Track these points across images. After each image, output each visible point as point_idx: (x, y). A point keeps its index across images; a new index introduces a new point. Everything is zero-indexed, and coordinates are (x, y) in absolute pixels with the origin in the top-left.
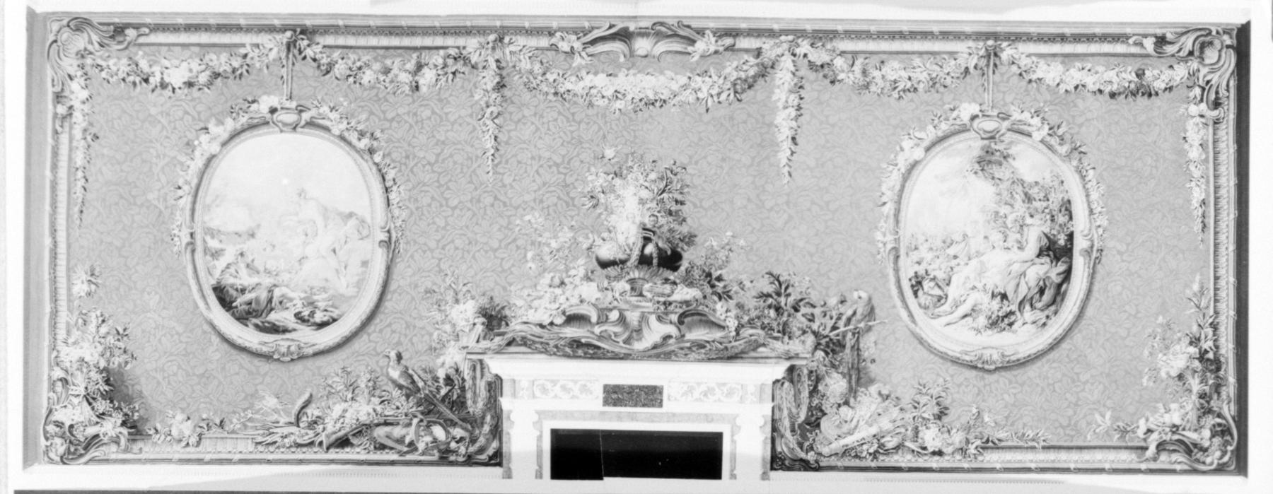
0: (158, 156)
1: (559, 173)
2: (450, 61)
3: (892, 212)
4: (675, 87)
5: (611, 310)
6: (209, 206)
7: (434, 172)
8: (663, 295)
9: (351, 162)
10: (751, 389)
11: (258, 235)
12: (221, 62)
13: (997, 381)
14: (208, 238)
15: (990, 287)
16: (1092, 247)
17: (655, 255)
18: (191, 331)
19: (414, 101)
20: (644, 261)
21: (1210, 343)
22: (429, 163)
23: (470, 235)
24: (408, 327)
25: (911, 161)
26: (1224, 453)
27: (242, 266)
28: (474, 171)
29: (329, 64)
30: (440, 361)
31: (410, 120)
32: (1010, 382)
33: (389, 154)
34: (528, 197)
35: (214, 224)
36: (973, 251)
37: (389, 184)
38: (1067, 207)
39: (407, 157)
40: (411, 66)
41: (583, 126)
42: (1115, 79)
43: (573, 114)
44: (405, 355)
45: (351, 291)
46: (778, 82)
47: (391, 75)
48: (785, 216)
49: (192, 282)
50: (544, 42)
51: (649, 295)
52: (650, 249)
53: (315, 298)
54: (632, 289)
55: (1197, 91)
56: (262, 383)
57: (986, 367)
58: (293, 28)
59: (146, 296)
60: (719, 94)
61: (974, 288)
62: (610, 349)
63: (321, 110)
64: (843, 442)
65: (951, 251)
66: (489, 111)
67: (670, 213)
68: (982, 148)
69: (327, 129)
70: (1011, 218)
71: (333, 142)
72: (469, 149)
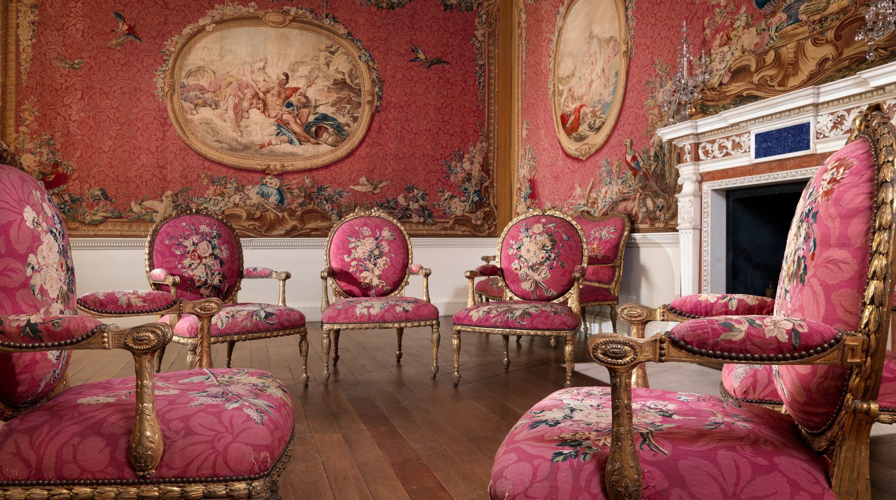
5: (767, 52)
8: (818, 11)
23: (669, 22)
30: (652, 141)
51: (803, 17)
54: (789, 17)
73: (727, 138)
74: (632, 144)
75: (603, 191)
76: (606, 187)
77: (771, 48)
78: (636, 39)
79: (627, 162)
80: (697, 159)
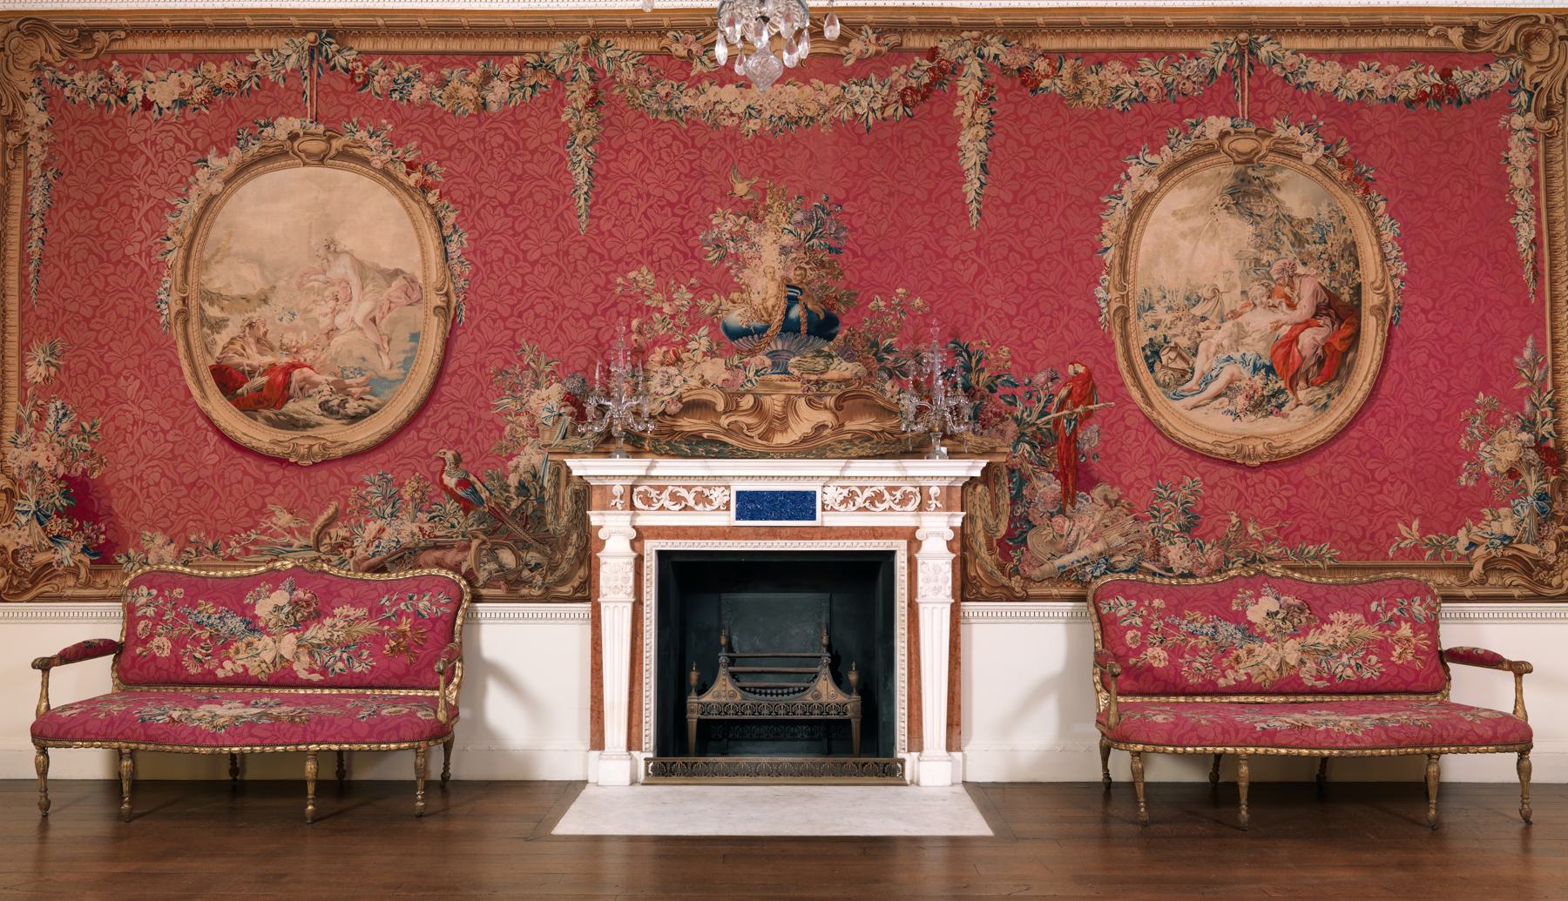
0: (141, 198)
1: (675, 215)
2: (528, 72)
3: (1117, 261)
4: (824, 100)
5: (743, 395)
6: (207, 263)
7: (507, 215)
9: (396, 202)
10: (934, 491)
11: (273, 301)
12: (225, 74)
13: (1263, 482)
14: (206, 305)
15: (1250, 356)
16: (1387, 303)
17: (803, 320)
18: (182, 427)
19: (480, 124)
20: (789, 327)
21: (1549, 427)
22: (501, 205)
23: (555, 297)
24: (471, 420)
25: (1141, 192)
27: (251, 340)
28: (561, 215)
29: (366, 76)
30: (512, 463)
31: (476, 149)
32: (1282, 483)
33: (448, 193)
34: (631, 248)
35: (216, 285)
36: (1227, 310)
37: (446, 232)
38: (1351, 251)
39: (472, 197)
40: (474, 77)
41: (706, 152)
42: (1413, 82)
43: (693, 138)
44: (467, 457)
45: (396, 373)
46: (960, 92)
48: (974, 268)
49: (184, 364)
50: (652, 45)
51: (796, 372)
52: (796, 312)
53: (347, 382)
54: (774, 364)
55: (1523, 97)
56: (271, 494)
57: (1248, 462)
58: (317, 29)
59: (122, 381)
60: (883, 108)
61: (1229, 359)
62: (742, 446)
64: (1058, 563)
65: (1197, 311)
66: (580, 136)
67: (822, 264)
68: (1236, 175)
69: (365, 161)
70: (1276, 266)
72: (554, 185)
73: (689, 488)
74: (458, 460)
75: (372, 527)
76: (380, 523)
77: (748, 392)
78: (472, 296)
79: (445, 488)
80: (632, 507)
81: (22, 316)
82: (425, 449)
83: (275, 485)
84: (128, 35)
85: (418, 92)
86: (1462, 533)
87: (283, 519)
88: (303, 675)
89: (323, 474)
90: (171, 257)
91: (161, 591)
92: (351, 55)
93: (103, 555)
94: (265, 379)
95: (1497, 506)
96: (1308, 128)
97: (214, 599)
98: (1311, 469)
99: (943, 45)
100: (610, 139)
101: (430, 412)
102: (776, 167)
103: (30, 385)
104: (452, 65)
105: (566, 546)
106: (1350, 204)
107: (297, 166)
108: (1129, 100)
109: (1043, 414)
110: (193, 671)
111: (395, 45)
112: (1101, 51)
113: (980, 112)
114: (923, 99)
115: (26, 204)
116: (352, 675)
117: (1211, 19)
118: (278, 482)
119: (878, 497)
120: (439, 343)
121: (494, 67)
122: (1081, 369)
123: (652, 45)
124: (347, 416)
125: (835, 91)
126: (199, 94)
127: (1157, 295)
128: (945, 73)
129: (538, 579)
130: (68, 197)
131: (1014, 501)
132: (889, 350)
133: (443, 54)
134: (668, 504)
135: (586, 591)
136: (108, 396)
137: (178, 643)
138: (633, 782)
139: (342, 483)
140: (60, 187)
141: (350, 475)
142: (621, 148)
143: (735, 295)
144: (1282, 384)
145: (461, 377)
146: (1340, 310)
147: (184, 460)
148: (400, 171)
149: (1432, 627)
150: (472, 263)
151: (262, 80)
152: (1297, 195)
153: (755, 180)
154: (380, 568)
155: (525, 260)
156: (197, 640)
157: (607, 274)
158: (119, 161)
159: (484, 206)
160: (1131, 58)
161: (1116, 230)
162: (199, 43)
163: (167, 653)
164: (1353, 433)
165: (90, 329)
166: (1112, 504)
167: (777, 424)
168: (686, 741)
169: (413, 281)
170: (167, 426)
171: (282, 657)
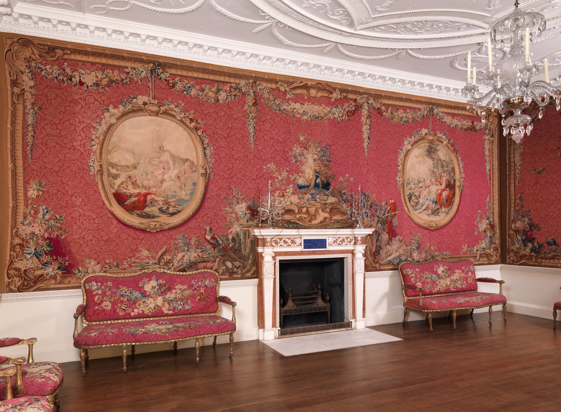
0: (80, 122)
2: (233, 90)
4: (326, 112)
5: (303, 207)
7: (226, 141)
8: (323, 200)
10: (359, 239)
11: (138, 168)
12: (116, 75)
14: (110, 168)
15: (432, 199)
18: (101, 217)
19: (216, 107)
20: (316, 186)
22: (224, 137)
23: (243, 172)
24: (215, 215)
26: (497, 257)
27: (130, 183)
28: (245, 143)
29: (173, 83)
30: (230, 231)
31: (215, 116)
33: (205, 131)
34: (268, 156)
38: (453, 169)
39: (214, 133)
41: (291, 125)
44: (214, 229)
45: (188, 198)
46: (363, 114)
47: (205, 92)
50: (274, 86)
53: (169, 200)
55: (488, 131)
58: (154, 63)
59: (74, 198)
60: (342, 116)
61: (427, 199)
62: (303, 224)
63: (171, 106)
64: (388, 259)
65: (420, 185)
66: (251, 115)
67: (325, 166)
69: (174, 116)
70: (438, 173)
71: (177, 123)
73: (289, 239)
74: (211, 230)
75: (180, 255)
76: (183, 253)
78: (215, 170)
79: (206, 240)
81: (25, 169)
82: (199, 226)
83: (141, 240)
84: (71, 53)
85: (193, 92)
86: (475, 247)
87: (145, 253)
88: (166, 312)
89: (160, 235)
90: (94, 148)
91: (102, 284)
92: (168, 75)
93: (67, 270)
94: (136, 199)
95: (482, 240)
96: (445, 134)
97: (126, 285)
98: (445, 230)
99: (358, 98)
100: (261, 117)
101: (201, 212)
102: (312, 132)
103: (30, 199)
104: (206, 84)
105: (248, 259)
106: (453, 156)
107: (147, 115)
108: (404, 121)
109: (384, 214)
110: (121, 314)
111: (184, 73)
112: (398, 106)
113: (368, 120)
114: (353, 114)
115: (25, 120)
116: (185, 310)
117: (423, 100)
118: (143, 239)
119: (343, 241)
120: (203, 187)
121: (221, 87)
122: (393, 201)
123: (274, 86)
124: (169, 213)
125: (329, 109)
126: (105, 82)
127: (411, 180)
128: (359, 107)
129: (240, 272)
130: (45, 119)
131: (377, 241)
132: (344, 194)
133: (202, 79)
134: (283, 244)
135: (257, 274)
136: (67, 204)
137: (114, 304)
138: (275, 338)
139: (168, 239)
140: (41, 114)
141: (171, 236)
142: (264, 121)
143: (300, 174)
144: (439, 207)
145: (211, 199)
146: (451, 186)
147: (103, 231)
148: (187, 121)
149: (473, 273)
150: (214, 158)
151: (132, 80)
152: (443, 153)
153: (306, 136)
154: (183, 270)
155: (233, 158)
156: (122, 302)
157: (260, 165)
158: (69, 106)
159: (218, 137)
160: (405, 108)
161: (401, 160)
162: (104, 61)
163: (109, 308)
164: (454, 221)
165: (58, 176)
166: (401, 241)
167: (313, 217)
168: (289, 322)
169: (193, 163)
170: (95, 217)
171: (158, 306)
